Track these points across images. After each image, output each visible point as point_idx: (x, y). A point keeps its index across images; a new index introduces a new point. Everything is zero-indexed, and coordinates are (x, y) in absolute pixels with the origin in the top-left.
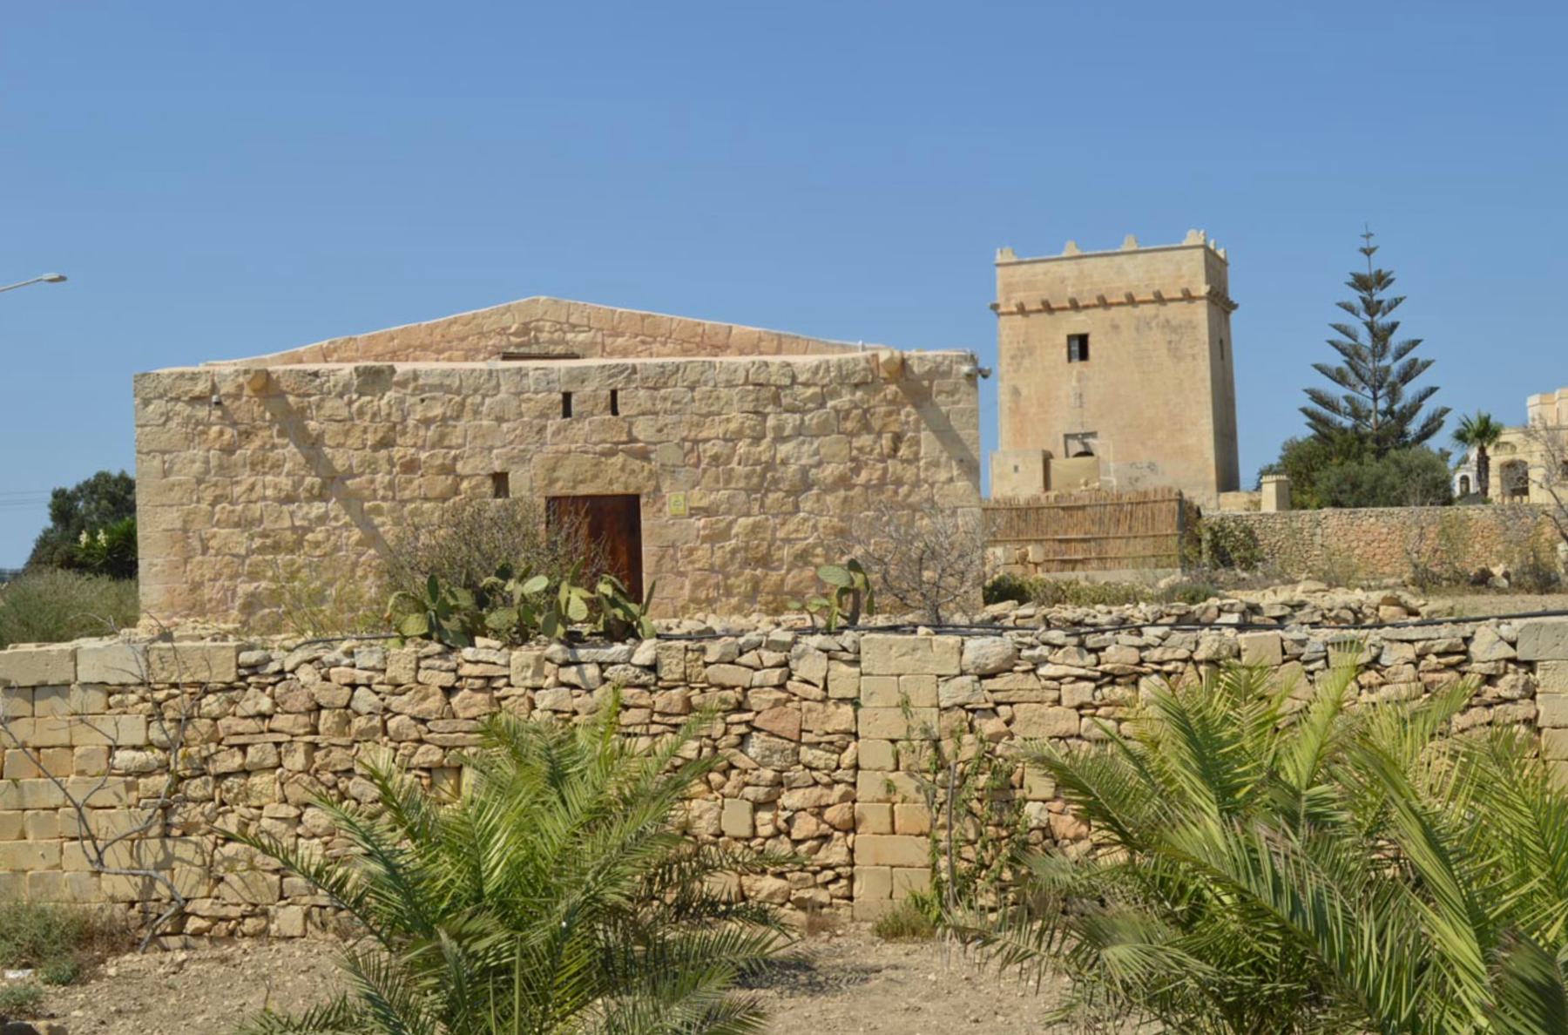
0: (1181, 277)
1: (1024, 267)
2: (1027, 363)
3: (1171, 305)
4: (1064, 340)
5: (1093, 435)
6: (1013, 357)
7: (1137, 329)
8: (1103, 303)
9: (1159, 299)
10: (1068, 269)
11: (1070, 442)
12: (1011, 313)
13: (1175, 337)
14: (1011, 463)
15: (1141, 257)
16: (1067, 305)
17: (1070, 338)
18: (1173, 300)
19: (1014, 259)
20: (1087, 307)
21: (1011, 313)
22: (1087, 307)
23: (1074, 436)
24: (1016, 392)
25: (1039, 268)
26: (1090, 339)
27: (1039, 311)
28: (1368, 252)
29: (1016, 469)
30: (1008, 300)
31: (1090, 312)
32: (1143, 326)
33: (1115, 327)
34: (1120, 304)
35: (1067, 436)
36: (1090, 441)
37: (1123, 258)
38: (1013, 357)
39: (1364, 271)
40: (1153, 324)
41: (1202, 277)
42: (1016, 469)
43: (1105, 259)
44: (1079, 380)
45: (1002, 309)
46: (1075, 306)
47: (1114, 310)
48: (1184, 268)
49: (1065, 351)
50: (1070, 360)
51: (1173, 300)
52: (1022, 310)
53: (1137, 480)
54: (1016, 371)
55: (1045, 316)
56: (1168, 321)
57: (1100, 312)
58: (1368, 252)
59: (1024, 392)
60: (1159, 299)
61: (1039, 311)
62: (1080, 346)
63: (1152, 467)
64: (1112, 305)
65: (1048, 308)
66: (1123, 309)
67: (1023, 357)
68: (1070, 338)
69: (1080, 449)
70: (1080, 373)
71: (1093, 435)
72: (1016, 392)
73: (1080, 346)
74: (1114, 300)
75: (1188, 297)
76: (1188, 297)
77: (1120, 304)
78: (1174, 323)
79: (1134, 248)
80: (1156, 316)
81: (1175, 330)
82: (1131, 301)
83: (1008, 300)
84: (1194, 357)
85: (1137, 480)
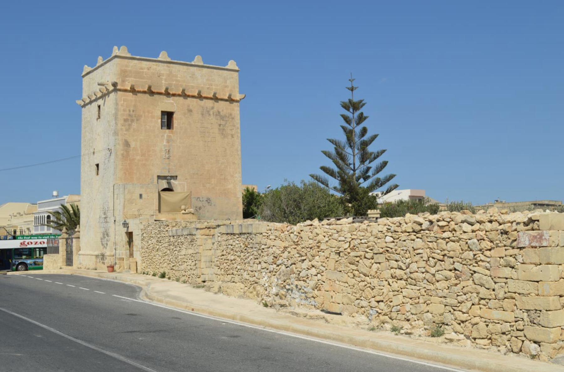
0: (226, 87)
1: (136, 61)
2: (135, 125)
3: (220, 102)
4: (160, 114)
5: (175, 177)
6: (126, 120)
7: (203, 114)
8: (184, 95)
9: (215, 99)
10: (162, 68)
11: (160, 180)
12: (126, 91)
13: (223, 123)
14: (138, 191)
15: (205, 70)
16: (163, 91)
17: (163, 113)
18: (222, 100)
19: (129, 55)
20: (174, 95)
21: (126, 91)
22: (174, 95)
23: (165, 178)
24: (127, 144)
25: (144, 63)
26: (174, 116)
27: (144, 92)
28: (352, 89)
29: (141, 196)
30: (123, 81)
31: (176, 98)
32: (205, 113)
33: (190, 111)
34: (193, 97)
35: (159, 177)
36: (172, 181)
37: (195, 68)
38: (126, 120)
39: (346, 97)
40: (211, 113)
41: (237, 90)
42: (141, 196)
43: (185, 67)
44: (168, 142)
45: (118, 87)
46: (167, 94)
47: (189, 99)
48: (228, 82)
49: (160, 121)
50: (162, 126)
51: (222, 100)
52: (133, 91)
53: (200, 208)
54: (127, 130)
55: (147, 95)
56: (219, 112)
57: (181, 99)
58: (352, 89)
59: (133, 144)
60: (215, 99)
61: (144, 92)
62: (168, 119)
63: (208, 201)
64: (189, 96)
65: (150, 92)
66: (195, 100)
67: (132, 121)
68: (163, 113)
69: (166, 186)
70: (168, 136)
71: (175, 177)
72: (127, 144)
73: (168, 119)
74: (191, 94)
75: (231, 100)
76: (231, 100)
77: (193, 97)
78: (221, 113)
79: (201, 64)
80: (213, 108)
81: (222, 118)
82: (200, 97)
83: (123, 81)
84: (232, 136)
85: (200, 208)
